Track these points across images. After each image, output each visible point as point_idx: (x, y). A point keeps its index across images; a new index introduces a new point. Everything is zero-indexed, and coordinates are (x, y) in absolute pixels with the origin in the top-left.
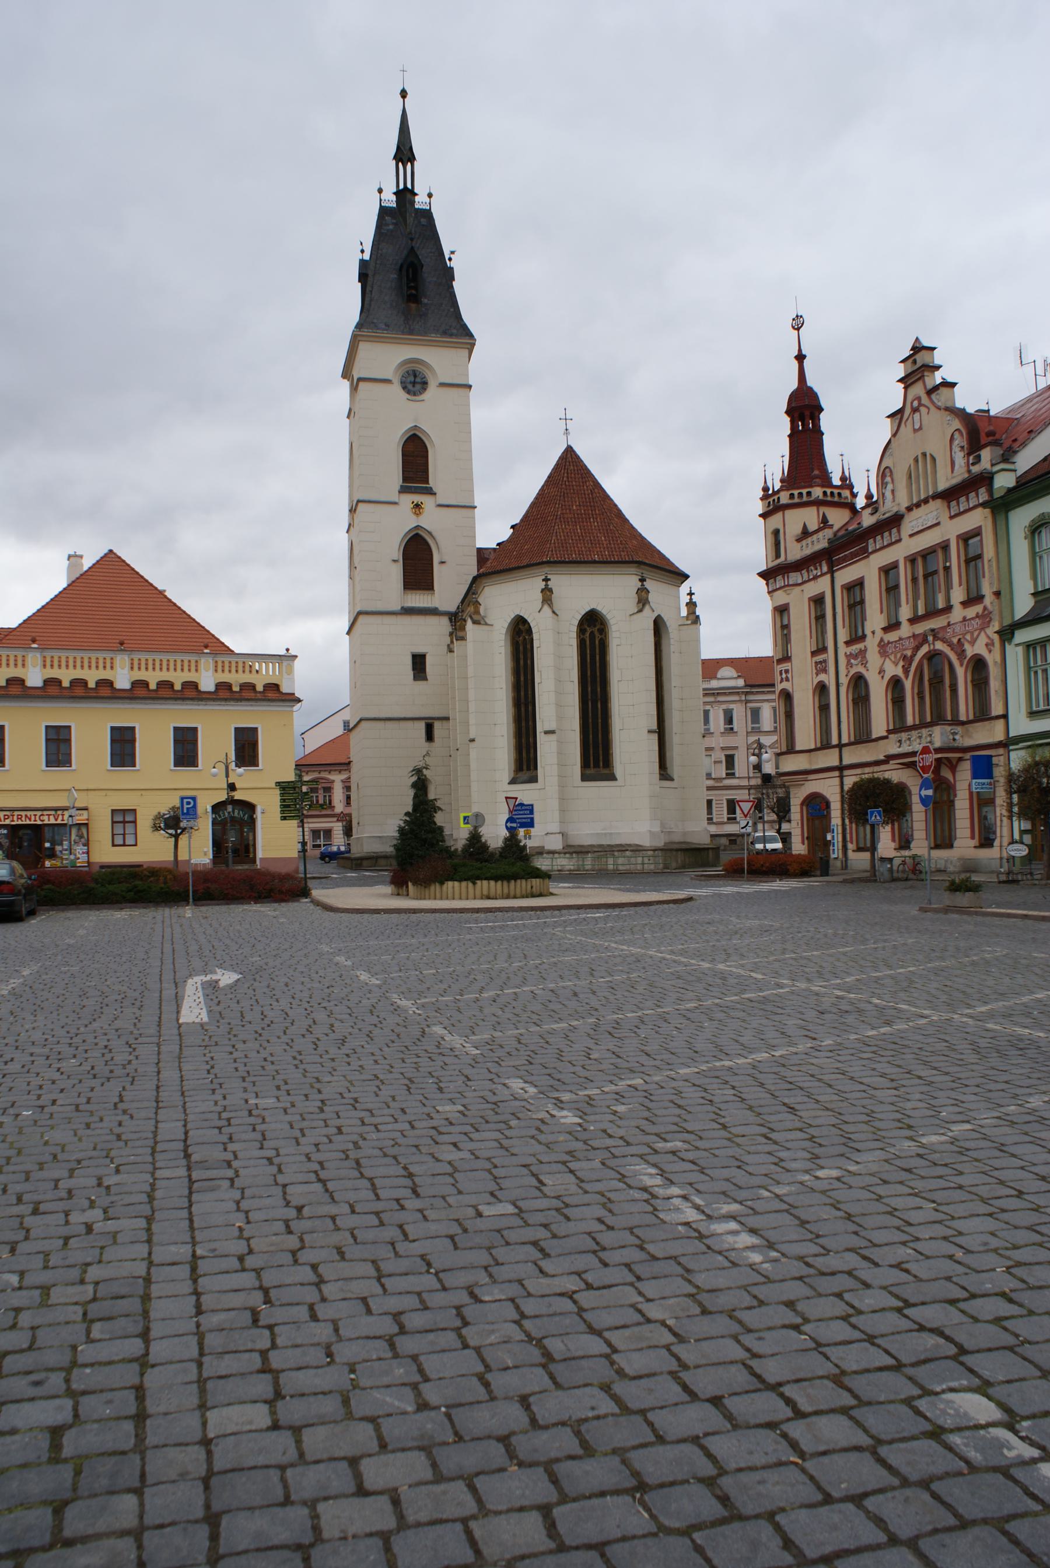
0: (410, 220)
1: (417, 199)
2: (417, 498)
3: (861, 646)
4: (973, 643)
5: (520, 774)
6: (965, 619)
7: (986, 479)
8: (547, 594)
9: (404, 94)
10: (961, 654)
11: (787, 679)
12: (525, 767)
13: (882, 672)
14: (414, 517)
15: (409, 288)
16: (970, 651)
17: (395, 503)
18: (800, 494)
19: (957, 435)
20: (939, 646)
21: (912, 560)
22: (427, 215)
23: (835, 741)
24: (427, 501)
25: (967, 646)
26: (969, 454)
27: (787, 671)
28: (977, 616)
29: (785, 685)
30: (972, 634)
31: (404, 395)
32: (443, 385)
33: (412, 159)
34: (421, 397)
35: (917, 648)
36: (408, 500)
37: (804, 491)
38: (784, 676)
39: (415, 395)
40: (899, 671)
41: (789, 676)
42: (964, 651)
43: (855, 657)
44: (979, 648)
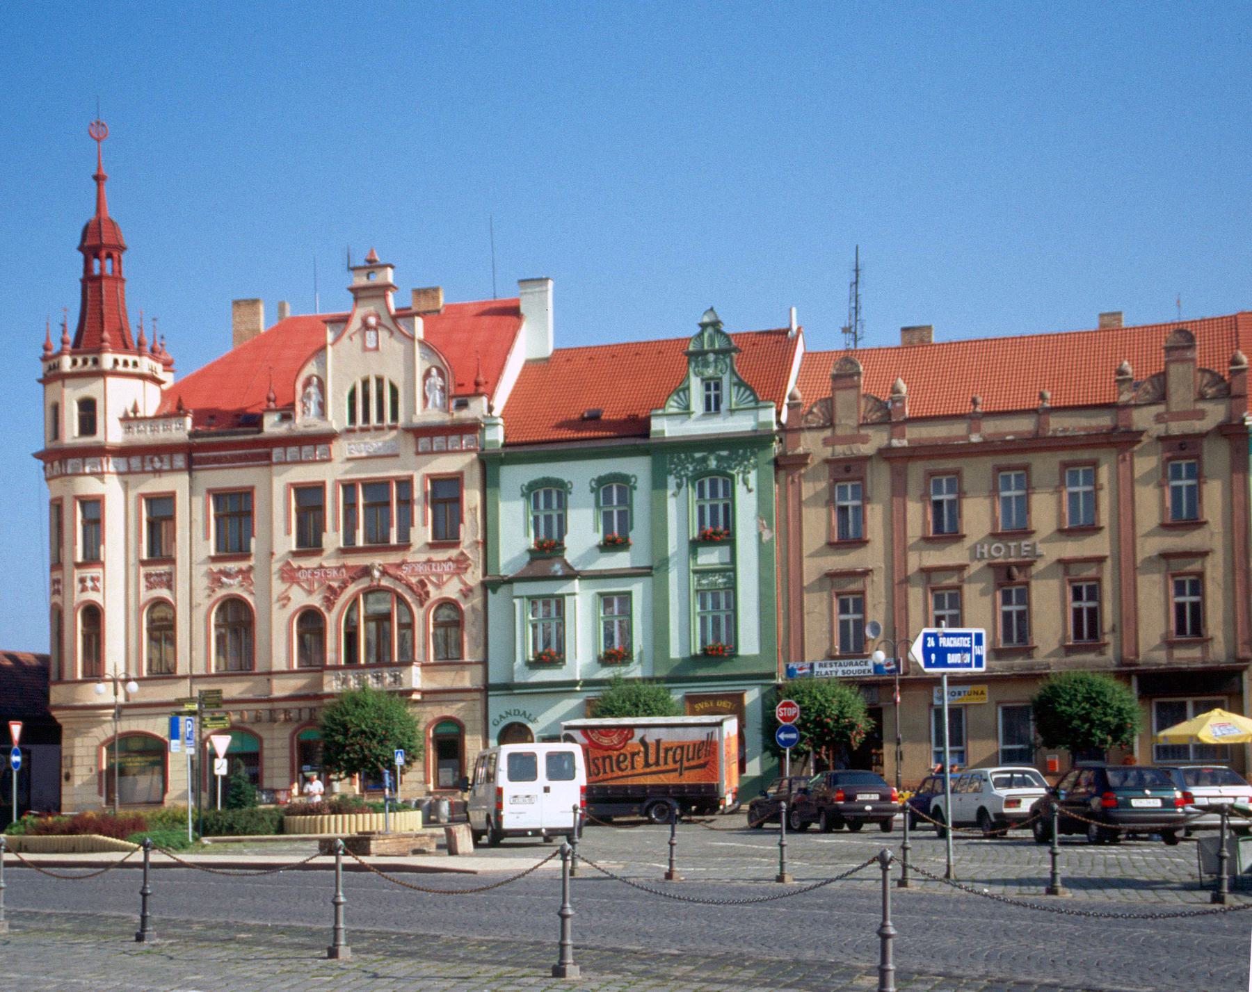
3: (244, 565)
6: (429, 561)
11: (95, 589)
16: (434, 594)
18: (126, 363)
21: (349, 487)
25: (430, 588)
27: (93, 579)
28: (450, 560)
29: (91, 596)
30: (439, 576)
40: (316, 601)
42: (427, 593)
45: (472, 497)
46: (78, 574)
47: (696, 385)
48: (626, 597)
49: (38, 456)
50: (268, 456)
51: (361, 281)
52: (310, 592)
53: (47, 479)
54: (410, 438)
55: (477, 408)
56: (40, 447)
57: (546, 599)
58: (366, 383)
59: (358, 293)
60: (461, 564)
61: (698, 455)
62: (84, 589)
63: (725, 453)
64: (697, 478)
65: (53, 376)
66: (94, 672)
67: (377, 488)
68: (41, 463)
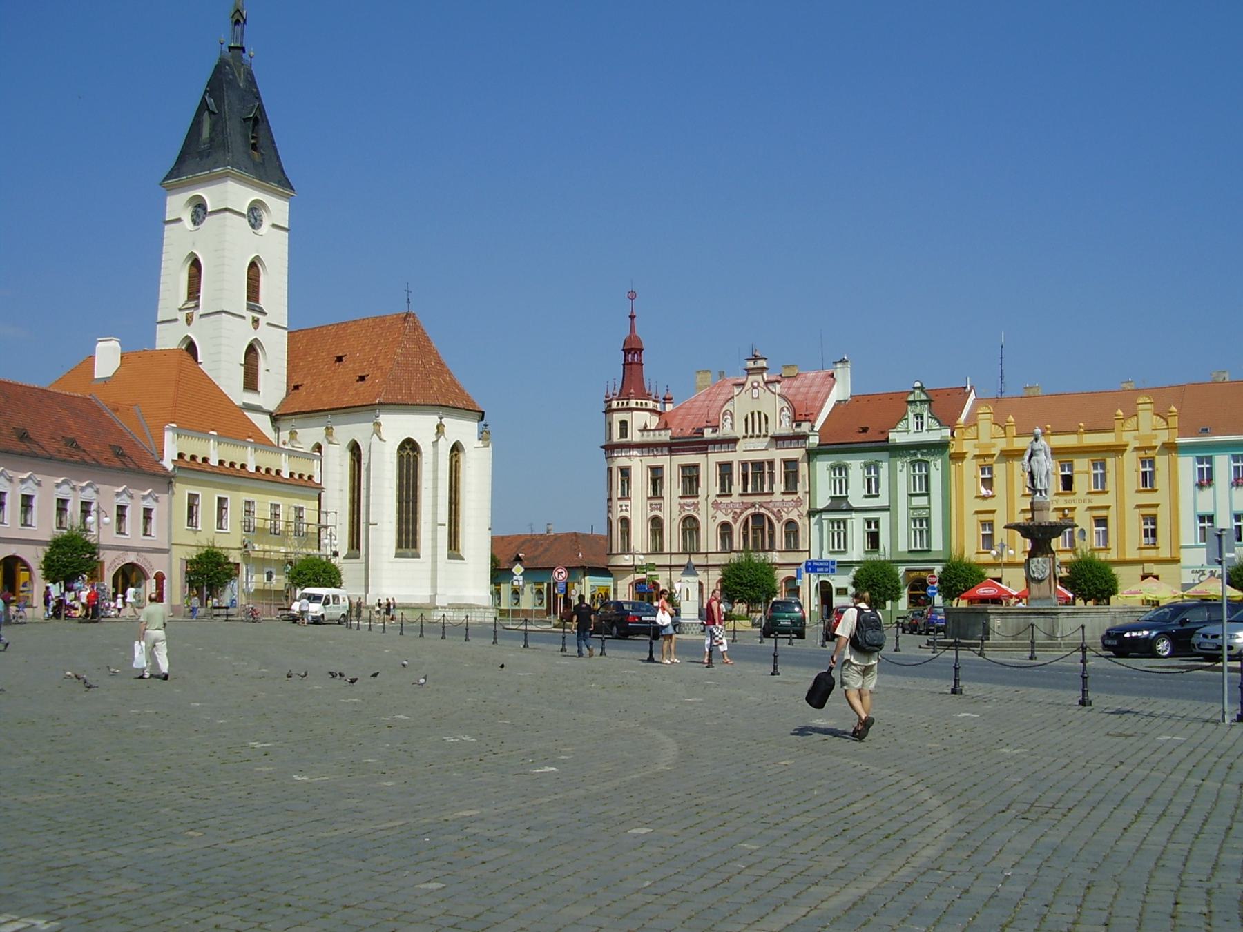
3: (695, 500)
4: (787, 513)
6: (783, 501)
7: (805, 437)
8: (440, 429)
10: (779, 519)
11: (627, 510)
13: (714, 517)
16: (786, 517)
18: (642, 404)
19: (785, 409)
20: (762, 511)
21: (744, 464)
23: (666, 550)
25: (783, 513)
26: (793, 422)
29: (627, 514)
30: (788, 508)
32: (274, 226)
35: (747, 509)
36: (250, 315)
37: (644, 402)
38: (624, 508)
40: (729, 519)
41: (629, 509)
43: (689, 506)
44: (793, 515)
45: (803, 468)
46: (620, 503)
47: (911, 416)
48: (877, 522)
49: (602, 447)
50: (707, 449)
51: (751, 364)
52: (726, 515)
53: (606, 458)
54: (774, 441)
55: (805, 427)
56: (603, 444)
57: (839, 522)
58: (753, 414)
59: (749, 371)
60: (798, 503)
61: (912, 452)
62: (622, 510)
63: (925, 451)
64: (913, 463)
65: (609, 411)
66: (627, 550)
67: (758, 465)
68: (604, 450)
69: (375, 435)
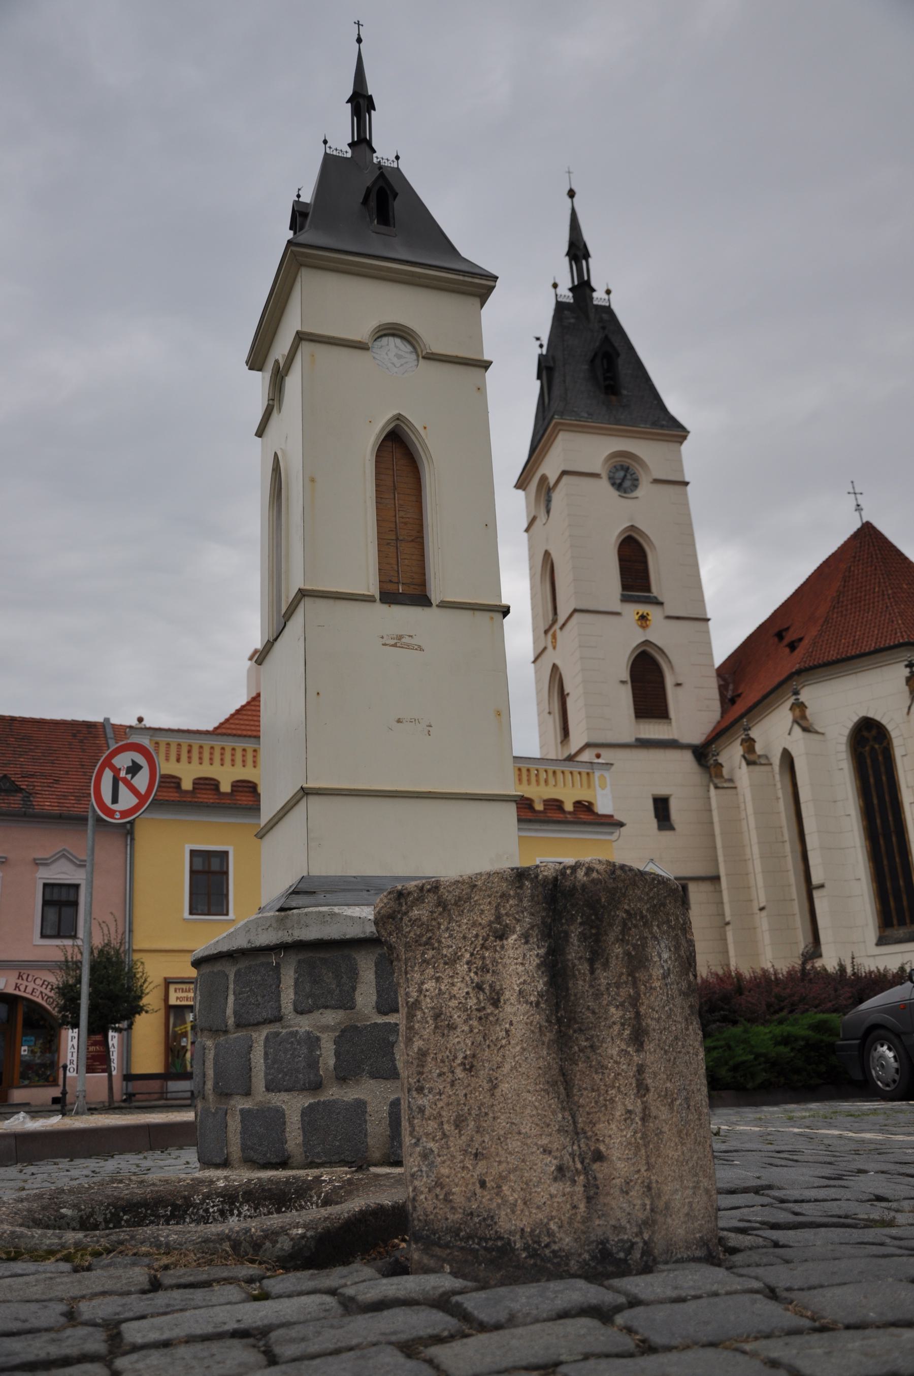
0: (592, 315)
1: (595, 295)
2: (643, 609)
5: (888, 932)
9: (571, 194)
12: (895, 922)
14: (640, 630)
15: (606, 379)
17: (618, 614)
22: (608, 311)
24: (653, 612)
31: (613, 493)
32: (656, 481)
33: (587, 256)
34: (634, 494)
36: (632, 611)
39: (625, 492)
69: (797, 729)
